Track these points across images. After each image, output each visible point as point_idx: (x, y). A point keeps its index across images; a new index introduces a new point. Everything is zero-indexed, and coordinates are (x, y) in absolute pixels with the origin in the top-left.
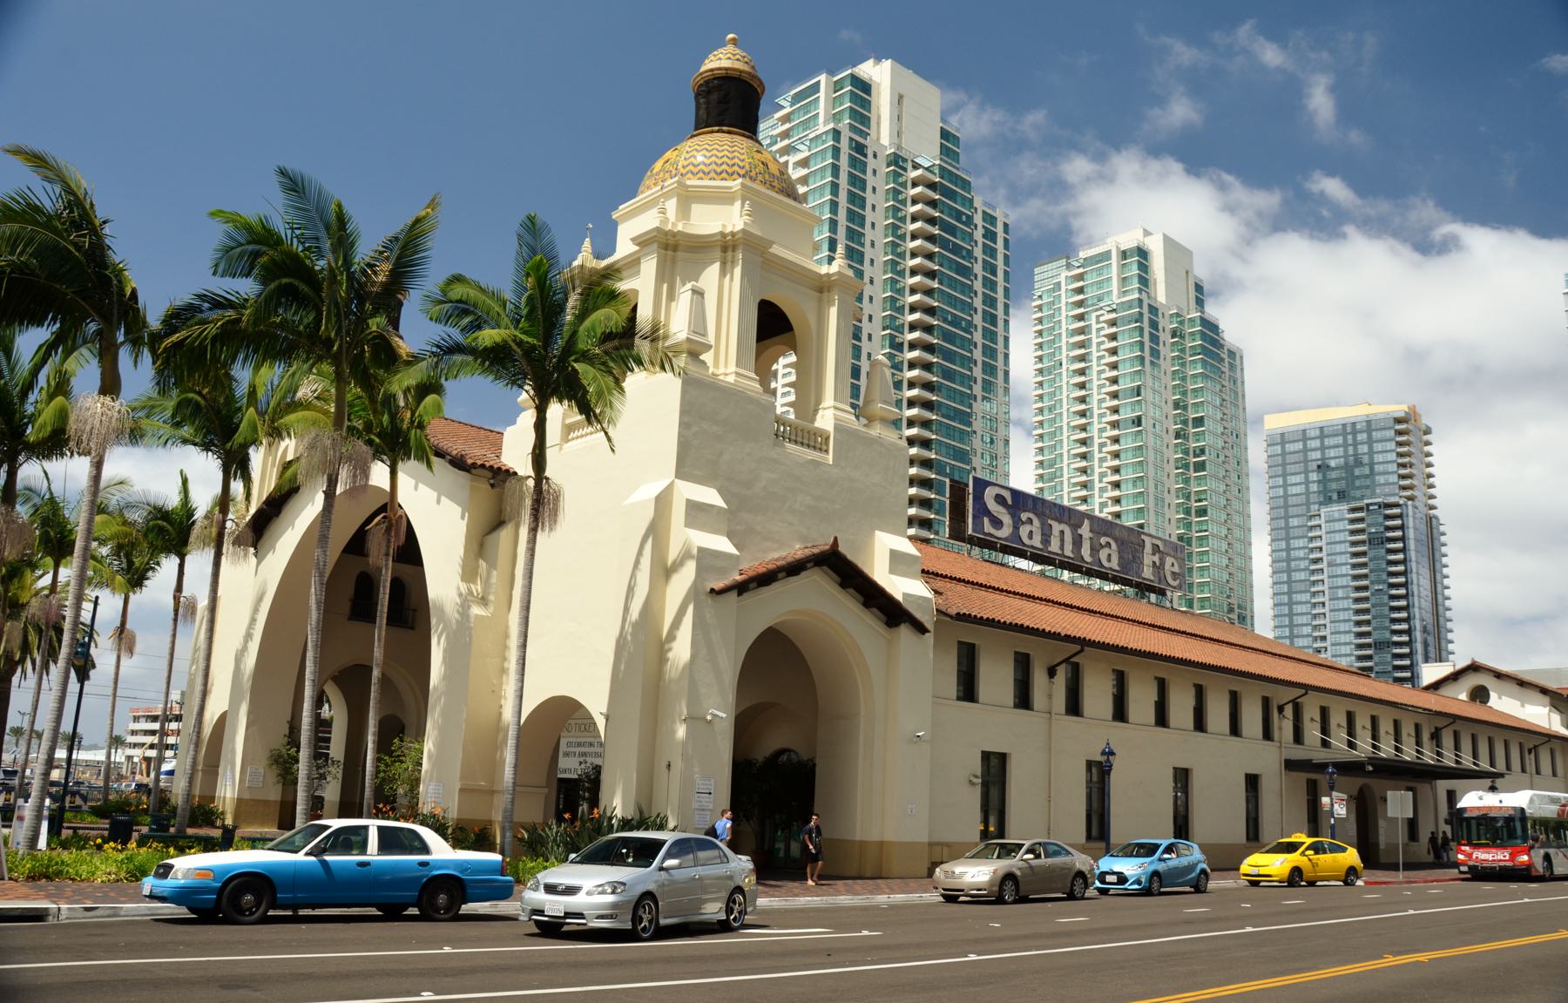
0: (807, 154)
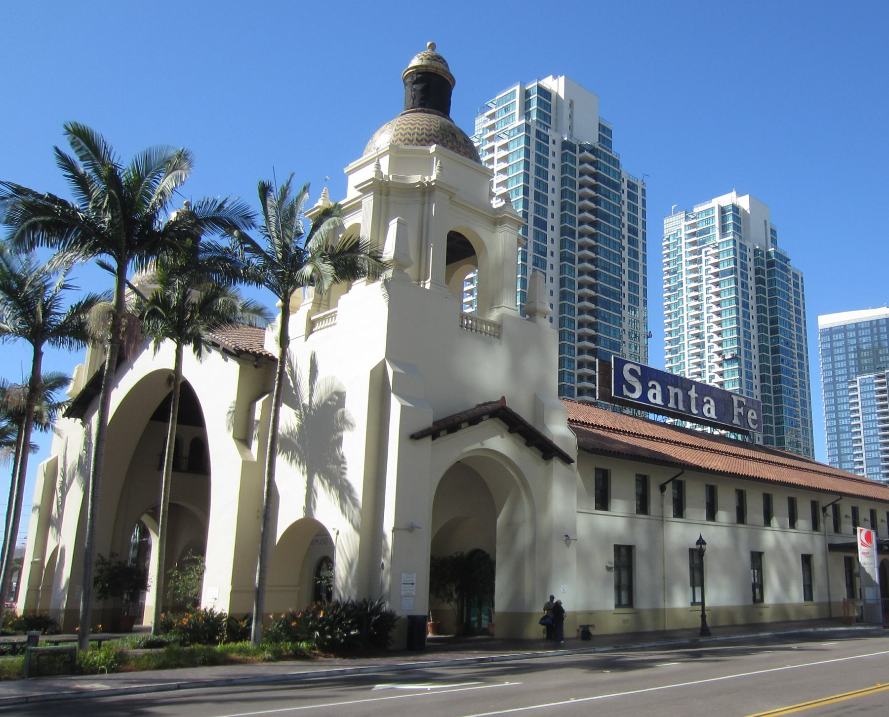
0: (507, 141)
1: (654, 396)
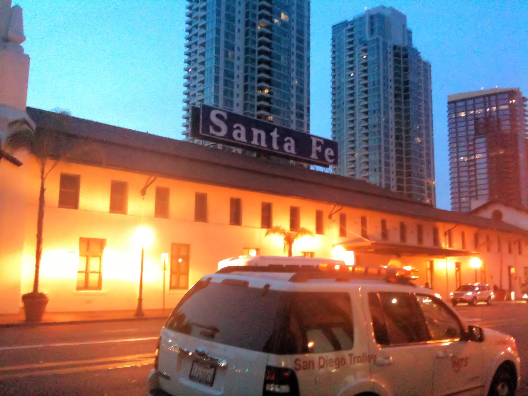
1: (239, 135)
